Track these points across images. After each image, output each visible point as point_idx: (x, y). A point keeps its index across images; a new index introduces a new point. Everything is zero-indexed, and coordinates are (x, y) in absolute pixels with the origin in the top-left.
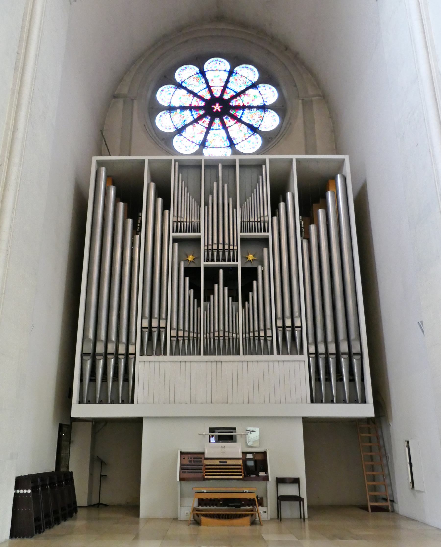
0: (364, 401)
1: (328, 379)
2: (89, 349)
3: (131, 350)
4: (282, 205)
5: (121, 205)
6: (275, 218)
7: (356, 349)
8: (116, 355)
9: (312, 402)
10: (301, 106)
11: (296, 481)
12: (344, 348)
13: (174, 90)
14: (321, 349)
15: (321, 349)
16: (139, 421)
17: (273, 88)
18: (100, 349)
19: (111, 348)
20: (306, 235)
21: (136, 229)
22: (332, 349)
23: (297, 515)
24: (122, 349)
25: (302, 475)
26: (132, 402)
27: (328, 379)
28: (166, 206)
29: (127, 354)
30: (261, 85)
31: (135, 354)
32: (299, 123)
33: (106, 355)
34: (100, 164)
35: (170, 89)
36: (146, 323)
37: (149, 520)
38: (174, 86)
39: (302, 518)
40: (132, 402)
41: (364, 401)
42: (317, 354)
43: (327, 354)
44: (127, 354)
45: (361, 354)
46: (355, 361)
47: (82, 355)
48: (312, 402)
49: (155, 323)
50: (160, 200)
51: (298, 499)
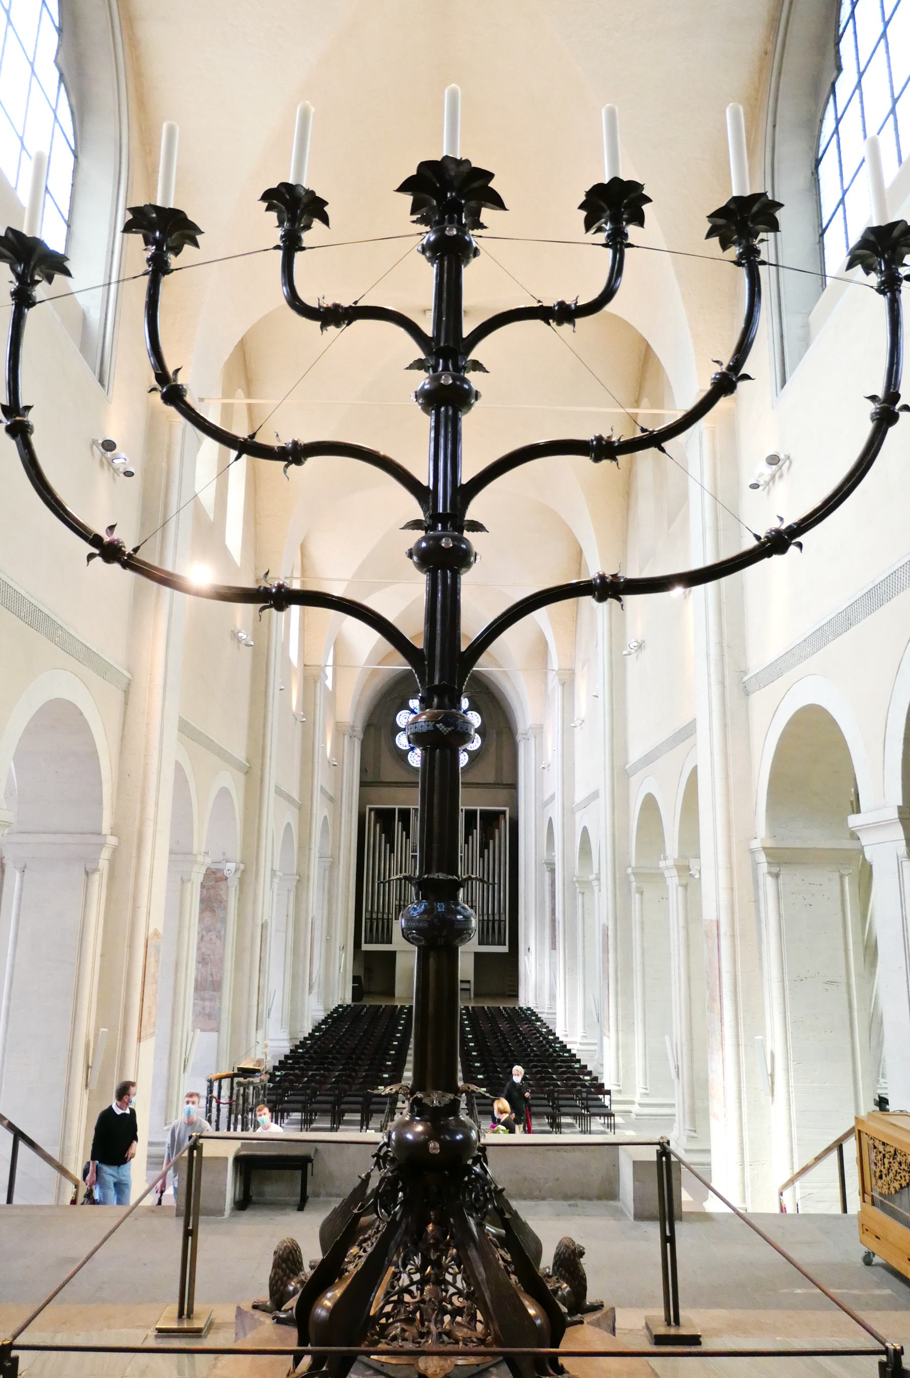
0: (505, 945)
1: (488, 932)
2: (368, 916)
3: (390, 917)
4: (470, 837)
5: (383, 835)
6: (466, 845)
7: (503, 918)
8: (383, 919)
9: (479, 944)
10: (495, 736)
11: (469, 982)
12: (497, 917)
13: (408, 715)
14: (486, 918)
15: (486, 918)
16: (393, 953)
17: (478, 716)
18: (375, 916)
19: (380, 916)
20: (482, 855)
21: (392, 851)
22: (491, 918)
23: (468, 997)
24: (386, 916)
25: (471, 978)
26: (391, 943)
27: (488, 932)
28: (408, 837)
29: (388, 919)
30: (469, 712)
31: (392, 919)
32: (493, 749)
33: (377, 919)
34: (371, 810)
35: (406, 714)
36: (397, 903)
37: (399, 998)
38: (408, 711)
39: (470, 999)
40: (391, 943)
41: (505, 945)
42: (483, 920)
43: (488, 920)
44: (388, 919)
45: (505, 921)
46: (502, 925)
47: (366, 919)
48: (479, 944)
49: (402, 903)
50: (404, 833)
51: (469, 990)
